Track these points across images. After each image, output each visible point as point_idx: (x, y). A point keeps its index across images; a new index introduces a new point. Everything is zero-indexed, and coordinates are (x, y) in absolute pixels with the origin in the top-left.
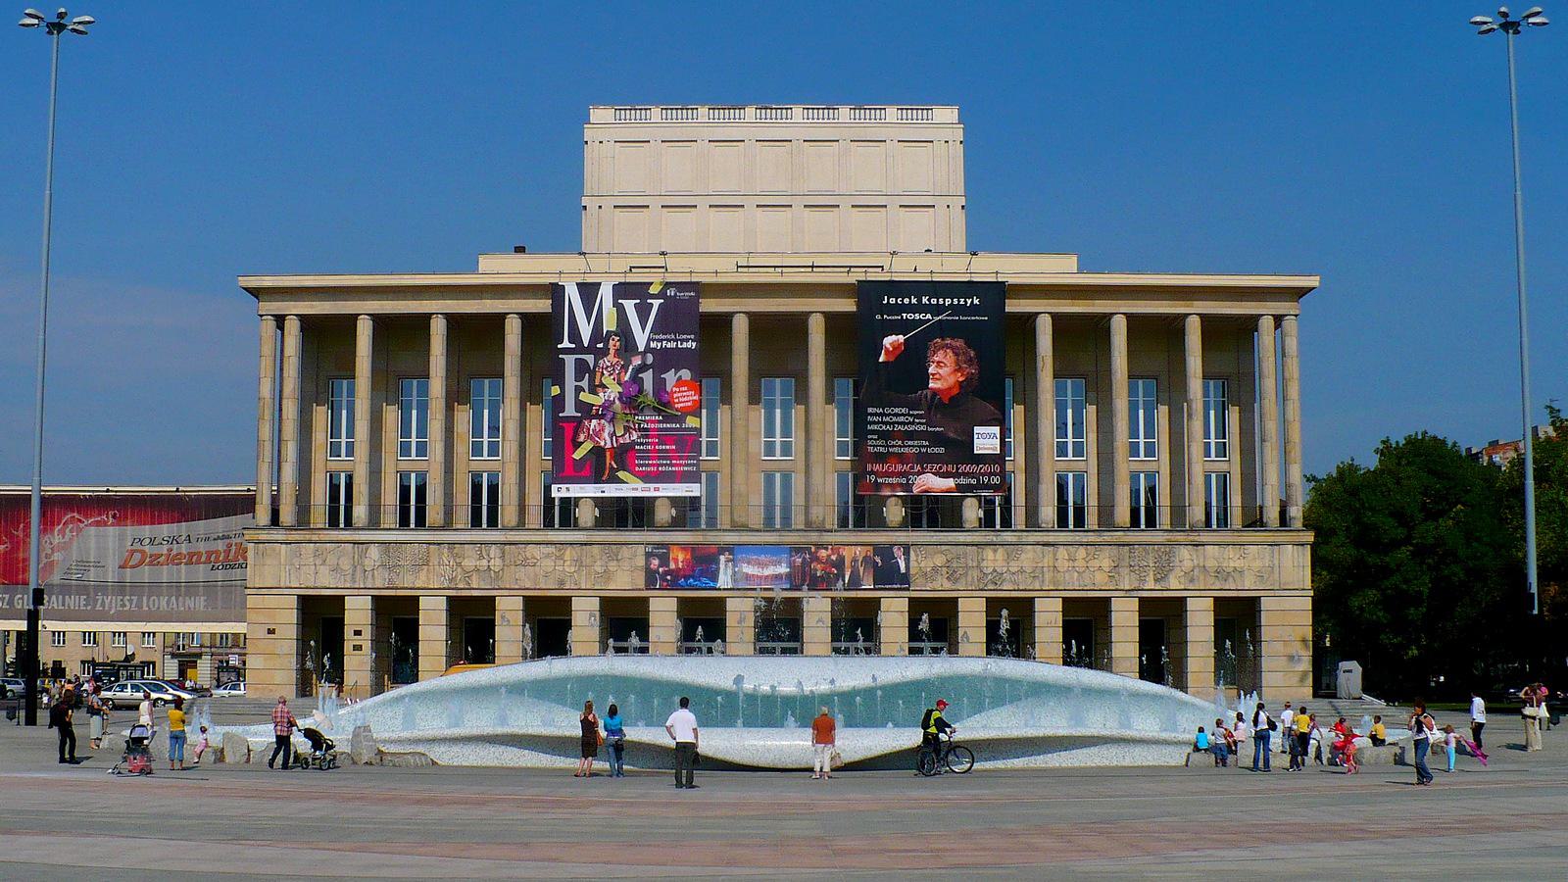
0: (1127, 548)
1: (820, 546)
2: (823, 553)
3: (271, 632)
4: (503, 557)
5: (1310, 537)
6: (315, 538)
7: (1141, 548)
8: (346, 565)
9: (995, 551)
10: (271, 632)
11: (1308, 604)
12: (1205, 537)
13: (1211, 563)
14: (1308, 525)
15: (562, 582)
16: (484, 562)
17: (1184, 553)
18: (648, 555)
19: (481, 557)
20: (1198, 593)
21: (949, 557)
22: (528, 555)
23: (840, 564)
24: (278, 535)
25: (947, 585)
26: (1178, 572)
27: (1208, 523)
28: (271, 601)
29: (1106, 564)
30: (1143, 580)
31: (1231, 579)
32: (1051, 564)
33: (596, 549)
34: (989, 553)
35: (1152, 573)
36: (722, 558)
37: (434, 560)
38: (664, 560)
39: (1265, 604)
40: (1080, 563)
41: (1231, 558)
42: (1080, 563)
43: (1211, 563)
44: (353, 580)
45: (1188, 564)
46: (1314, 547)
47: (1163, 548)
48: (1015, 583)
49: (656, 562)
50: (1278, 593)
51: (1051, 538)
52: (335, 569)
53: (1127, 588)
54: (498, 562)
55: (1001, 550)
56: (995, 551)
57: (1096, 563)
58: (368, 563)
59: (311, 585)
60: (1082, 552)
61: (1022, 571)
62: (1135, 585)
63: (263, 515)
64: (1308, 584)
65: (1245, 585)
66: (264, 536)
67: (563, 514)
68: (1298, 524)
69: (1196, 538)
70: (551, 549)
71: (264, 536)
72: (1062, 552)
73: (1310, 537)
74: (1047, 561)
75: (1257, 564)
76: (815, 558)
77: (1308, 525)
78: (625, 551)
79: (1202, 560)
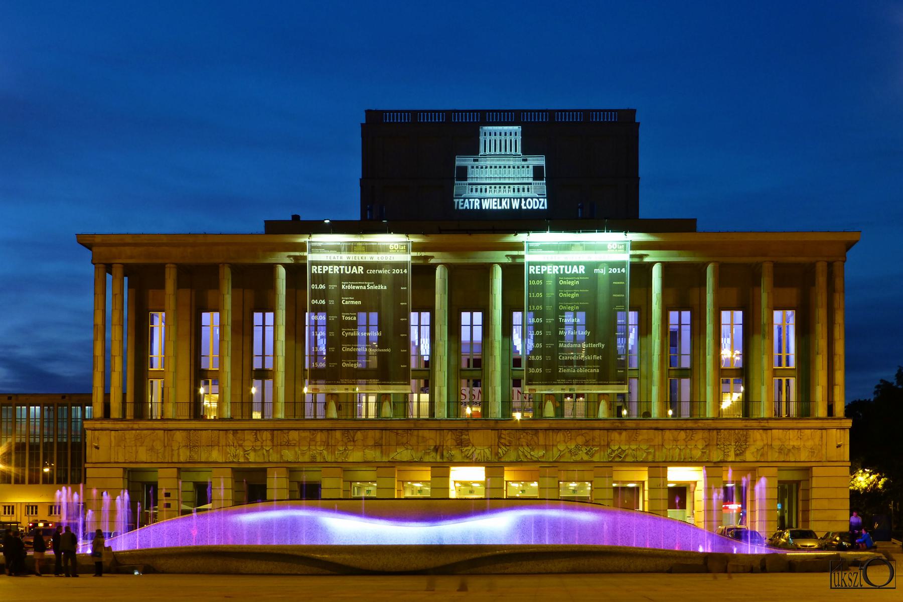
0: (715, 432)
4: (272, 440)
5: (849, 423)
6: (136, 426)
7: (726, 432)
8: (158, 446)
9: (620, 434)
13: (776, 444)
15: (314, 457)
16: (259, 443)
17: (757, 435)
19: (256, 439)
20: (766, 464)
21: (588, 438)
22: (291, 438)
24: (107, 424)
25: (586, 458)
26: (752, 449)
28: (103, 472)
30: (726, 454)
31: (791, 454)
32: (660, 443)
33: (338, 434)
35: (733, 450)
37: (223, 442)
41: (792, 439)
43: (776, 444)
44: (164, 456)
45: (759, 444)
46: (851, 430)
47: (741, 432)
48: (634, 456)
50: (825, 464)
52: (152, 449)
53: (715, 460)
54: (269, 443)
55: (624, 433)
56: (620, 434)
57: (693, 443)
59: (133, 460)
60: (682, 434)
63: (96, 409)
64: (847, 456)
66: (98, 425)
69: (766, 425)
70: (307, 434)
71: (98, 425)
73: (849, 423)
75: (810, 444)
78: (359, 435)
79: (770, 440)
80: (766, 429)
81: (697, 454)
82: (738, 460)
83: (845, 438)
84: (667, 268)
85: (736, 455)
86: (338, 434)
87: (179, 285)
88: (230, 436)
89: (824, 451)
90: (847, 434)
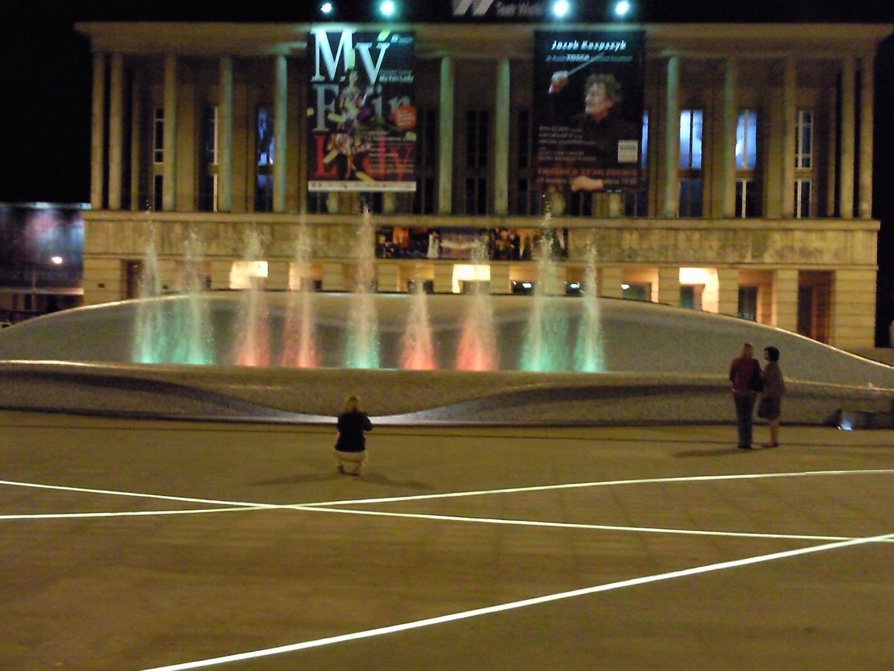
1: (502, 229)
2: (504, 234)
3: (101, 286)
5: (877, 225)
9: (631, 234)
10: (101, 286)
11: (872, 276)
12: (794, 224)
13: (797, 245)
14: (875, 215)
18: (378, 233)
23: (516, 241)
24: (105, 215)
26: (771, 251)
27: (795, 215)
28: (99, 264)
29: (716, 244)
33: (340, 230)
34: (627, 236)
36: (431, 237)
37: (222, 234)
38: (389, 238)
39: (840, 275)
40: (696, 244)
41: (814, 242)
42: (696, 244)
43: (797, 245)
46: (881, 234)
49: (382, 239)
51: (675, 224)
53: (731, 261)
56: (631, 234)
57: (706, 244)
58: (173, 236)
60: (696, 236)
61: (651, 249)
62: (737, 259)
65: (825, 261)
67: (317, 204)
68: (868, 215)
72: (682, 236)
73: (877, 225)
74: (671, 242)
76: (498, 237)
77: (875, 215)
80: (786, 230)
81: (711, 255)
82: (755, 261)
83: (873, 242)
84: (684, 65)
85: (754, 257)
86: (340, 230)
87: (181, 80)
88: (230, 229)
89: (849, 255)
90: (875, 238)
